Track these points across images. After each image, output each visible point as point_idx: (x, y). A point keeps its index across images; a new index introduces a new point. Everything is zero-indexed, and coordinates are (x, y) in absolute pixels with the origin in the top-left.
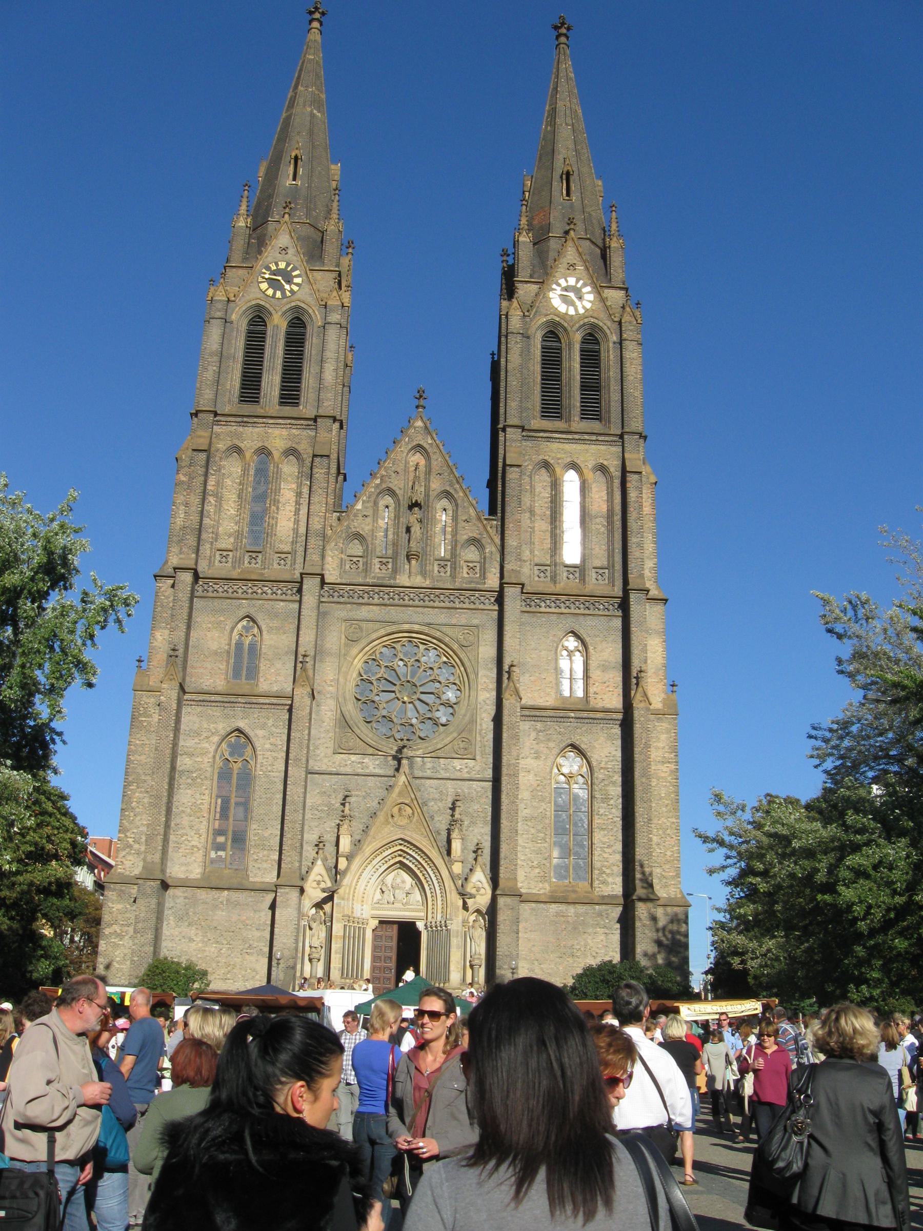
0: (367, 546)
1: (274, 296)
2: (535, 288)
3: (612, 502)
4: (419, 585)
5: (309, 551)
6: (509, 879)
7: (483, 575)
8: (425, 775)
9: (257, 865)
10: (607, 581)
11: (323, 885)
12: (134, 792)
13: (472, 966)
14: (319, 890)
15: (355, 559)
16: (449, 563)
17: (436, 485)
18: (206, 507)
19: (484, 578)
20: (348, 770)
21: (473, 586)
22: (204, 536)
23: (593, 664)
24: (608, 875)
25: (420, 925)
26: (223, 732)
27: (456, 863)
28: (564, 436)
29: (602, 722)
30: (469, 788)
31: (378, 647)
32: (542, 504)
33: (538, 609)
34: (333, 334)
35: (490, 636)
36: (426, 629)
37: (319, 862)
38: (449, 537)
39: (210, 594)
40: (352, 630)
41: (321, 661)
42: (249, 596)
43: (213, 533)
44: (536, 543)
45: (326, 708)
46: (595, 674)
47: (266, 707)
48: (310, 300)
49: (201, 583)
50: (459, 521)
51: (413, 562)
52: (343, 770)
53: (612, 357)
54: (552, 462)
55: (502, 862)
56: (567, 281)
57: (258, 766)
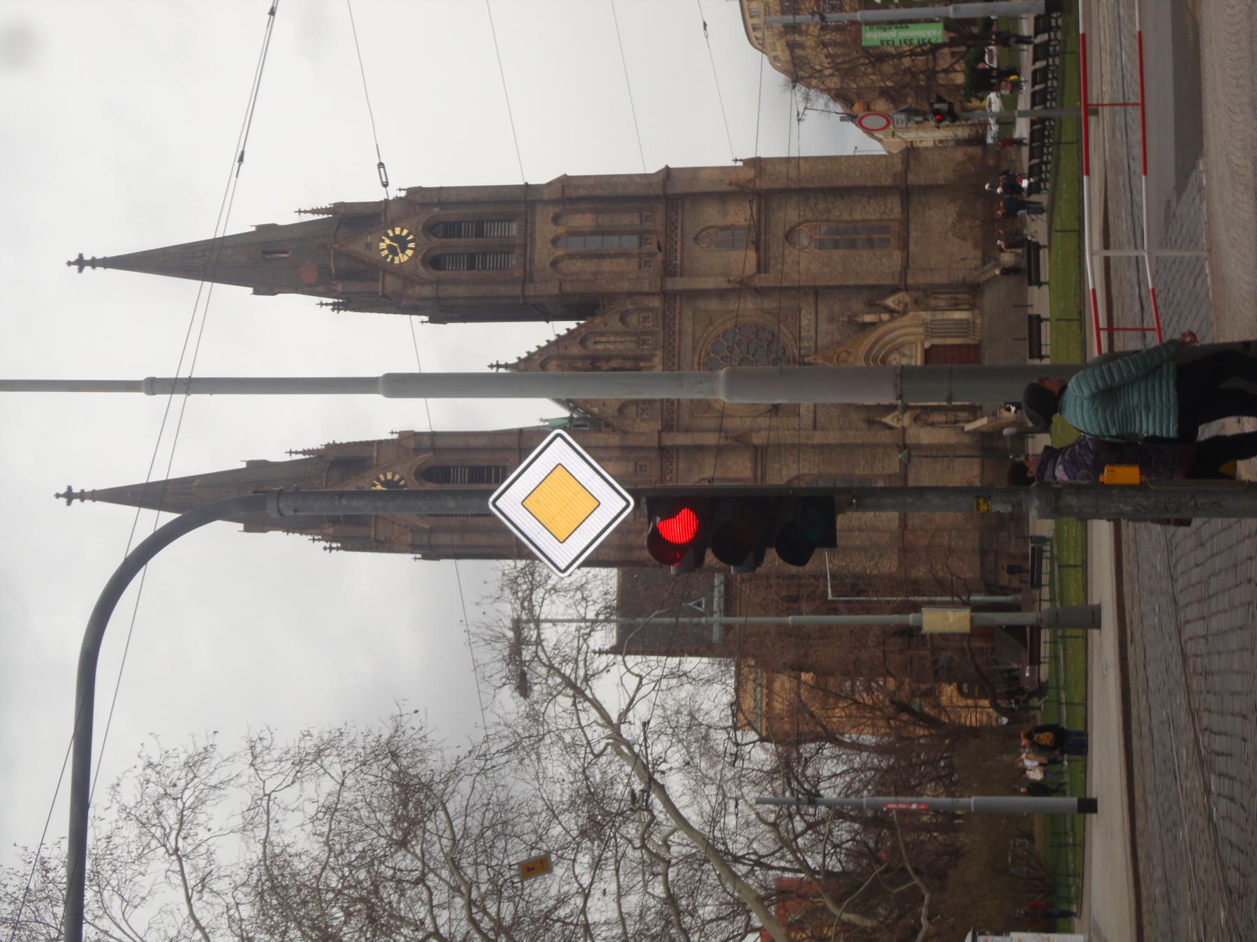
2: (388, 278)
7: (651, 310)
13: (957, 305)
21: (660, 317)
23: (722, 222)
25: (927, 345)
28: (528, 250)
32: (588, 267)
34: (440, 443)
35: (702, 304)
38: (618, 339)
46: (731, 220)
53: (454, 211)
54: (551, 258)
56: (383, 250)
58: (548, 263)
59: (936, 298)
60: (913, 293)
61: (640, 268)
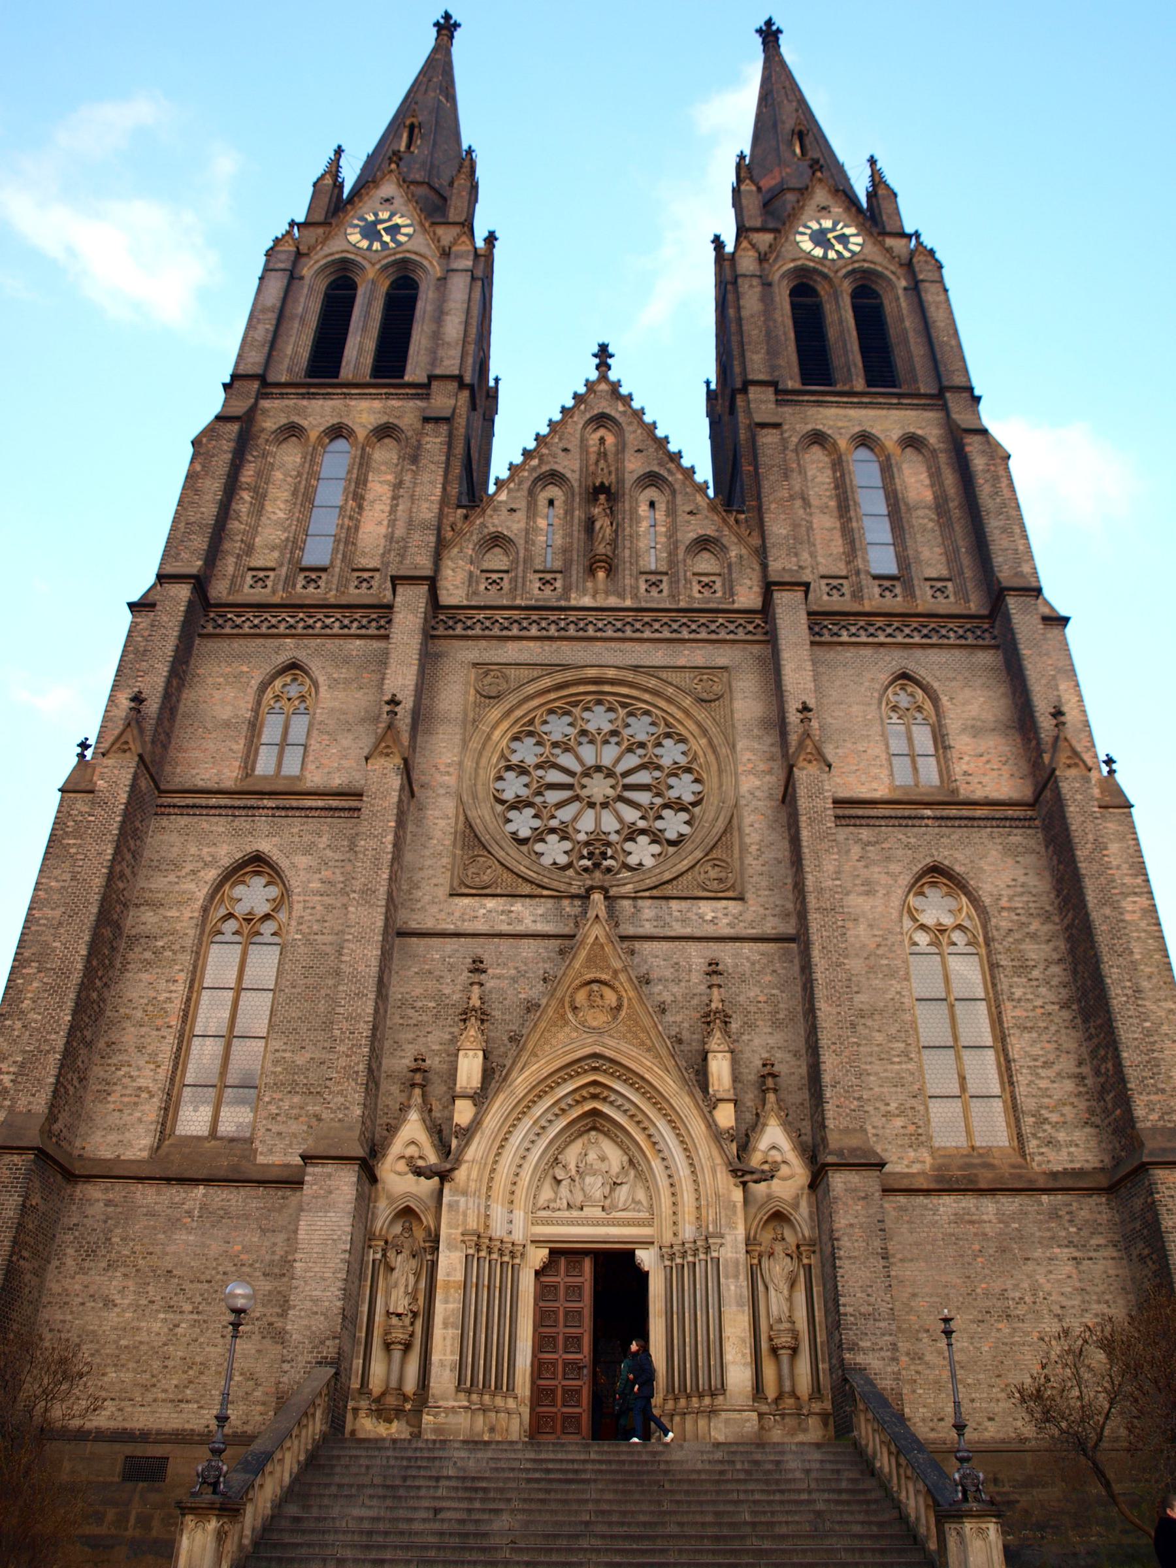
0: (517, 553)
1: (369, 248)
2: (768, 237)
3: (941, 485)
4: (613, 605)
5: (413, 550)
6: (847, 1131)
7: (730, 592)
8: (640, 931)
9: (275, 1128)
10: (952, 599)
11: (420, 1163)
12: (29, 979)
13: (774, 1351)
14: (410, 1176)
15: (495, 576)
16: (665, 578)
17: (634, 466)
18: (234, 506)
19: (732, 595)
20: (481, 927)
22: (227, 546)
23: (953, 724)
24: (1055, 1126)
25: (646, 1258)
26: (226, 862)
27: (721, 1106)
28: (845, 399)
29: (989, 823)
30: (736, 955)
31: (539, 712)
33: (835, 639)
34: (459, 286)
36: (630, 676)
37: (414, 1116)
38: (663, 540)
39: (228, 630)
40: (489, 679)
41: (429, 732)
42: (300, 631)
43: (242, 541)
44: (819, 546)
45: (437, 813)
46: (961, 742)
47: (313, 813)
48: (423, 250)
49: (212, 615)
50: (679, 512)
51: (601, 575)
52: (468, 927)
53: (904, 304)
54: (829, 432)
55: (828, 1093)
57: (293, 923)
58: (820, 427)
59: (792, 1286)
60: (804, 1208)
61: (823, 577)
